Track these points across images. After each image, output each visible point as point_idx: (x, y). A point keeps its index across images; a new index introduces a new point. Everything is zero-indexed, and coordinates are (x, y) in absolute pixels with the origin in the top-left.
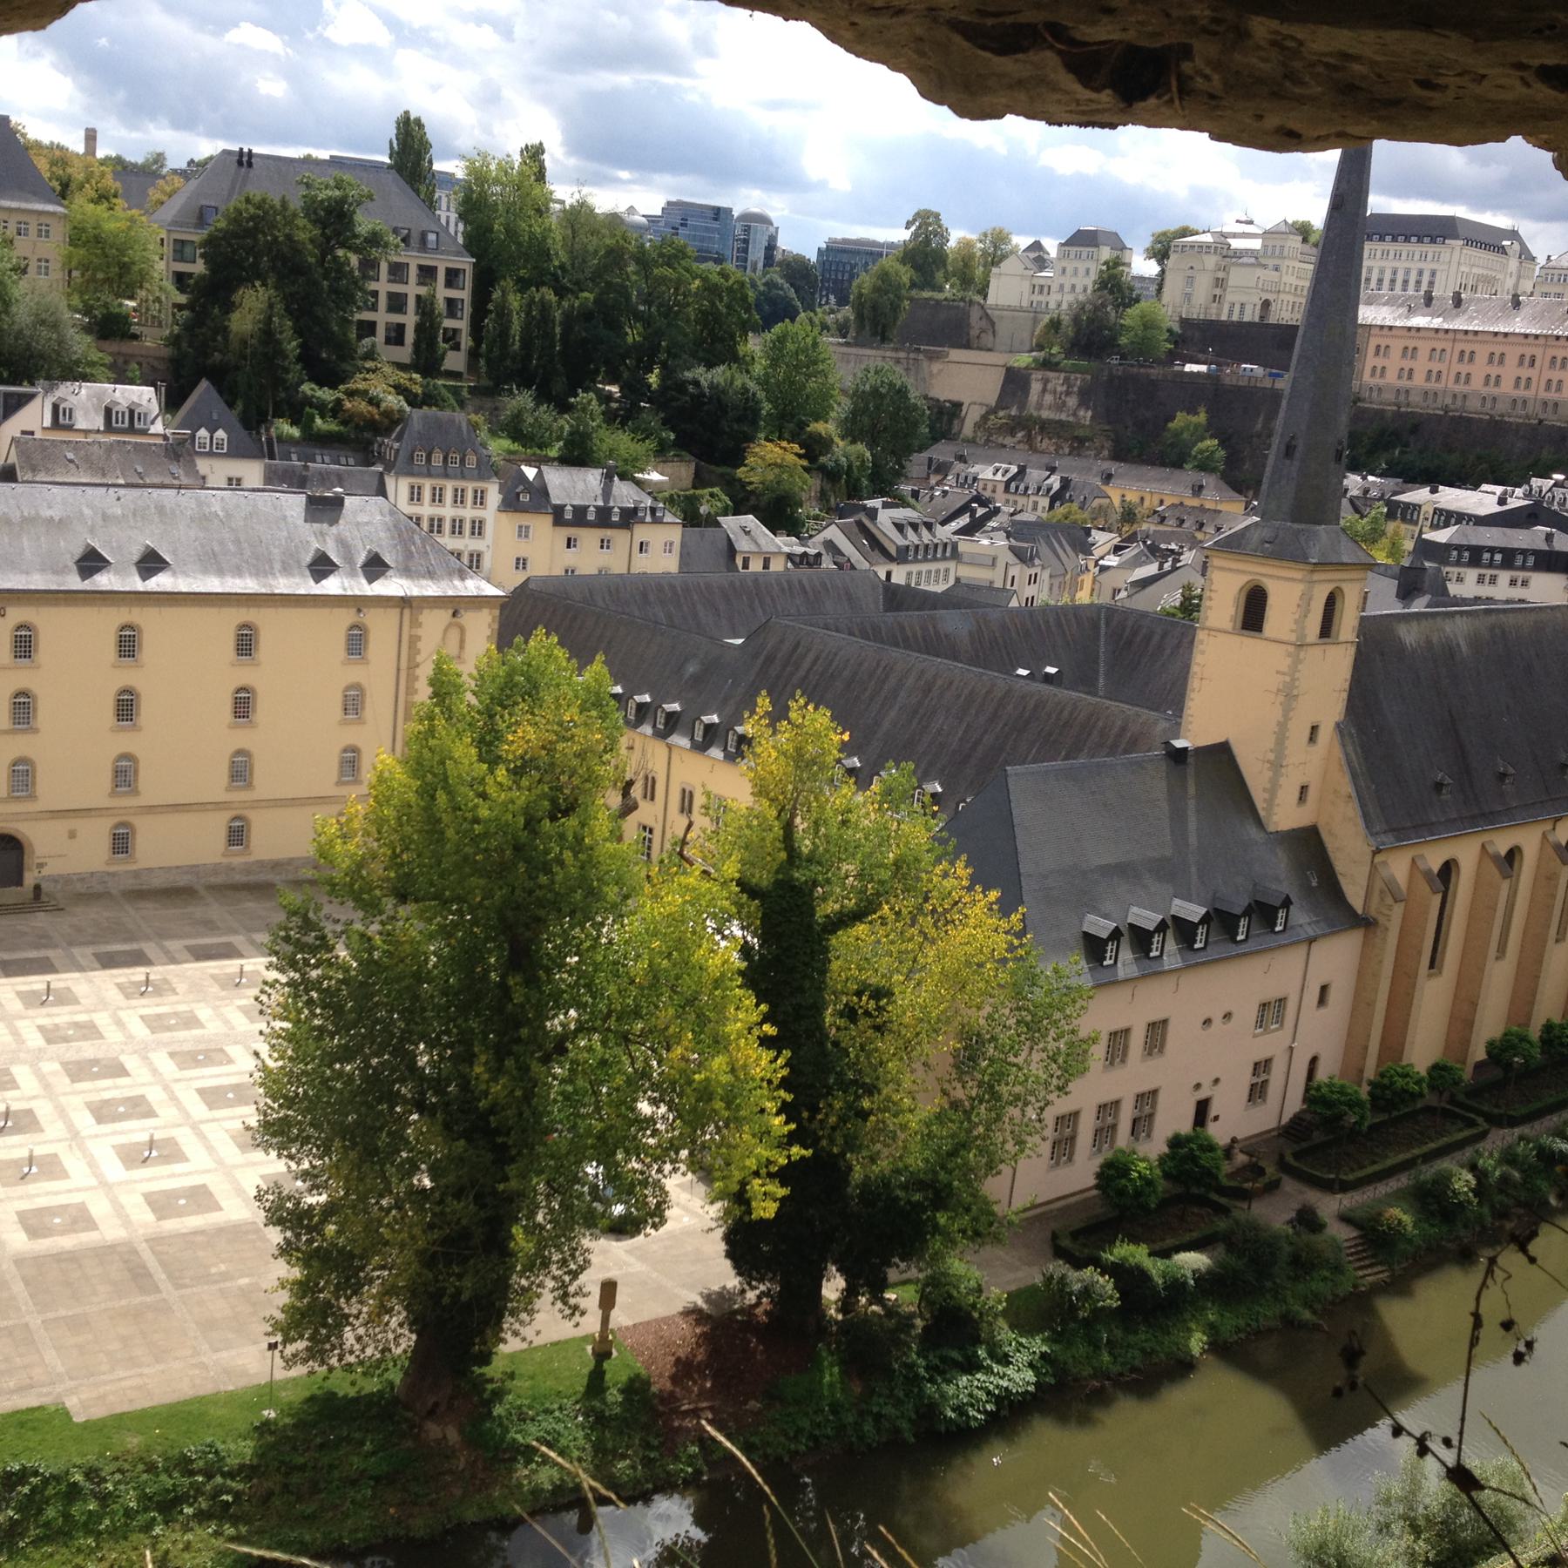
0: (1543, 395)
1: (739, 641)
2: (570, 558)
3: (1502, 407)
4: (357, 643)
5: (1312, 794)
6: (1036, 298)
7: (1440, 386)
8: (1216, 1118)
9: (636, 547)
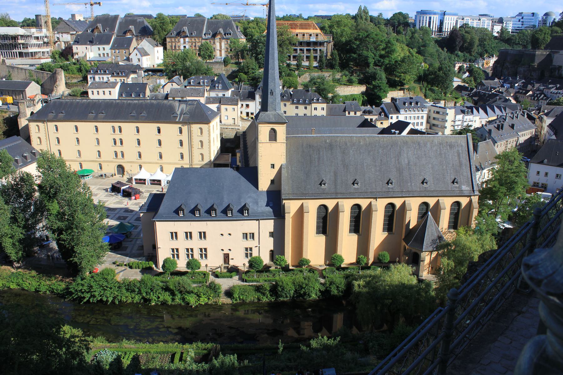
2: (296, 111)
4: (181, 132)
5: (275, 182)
8: (232, 259)
9: (313, 109)
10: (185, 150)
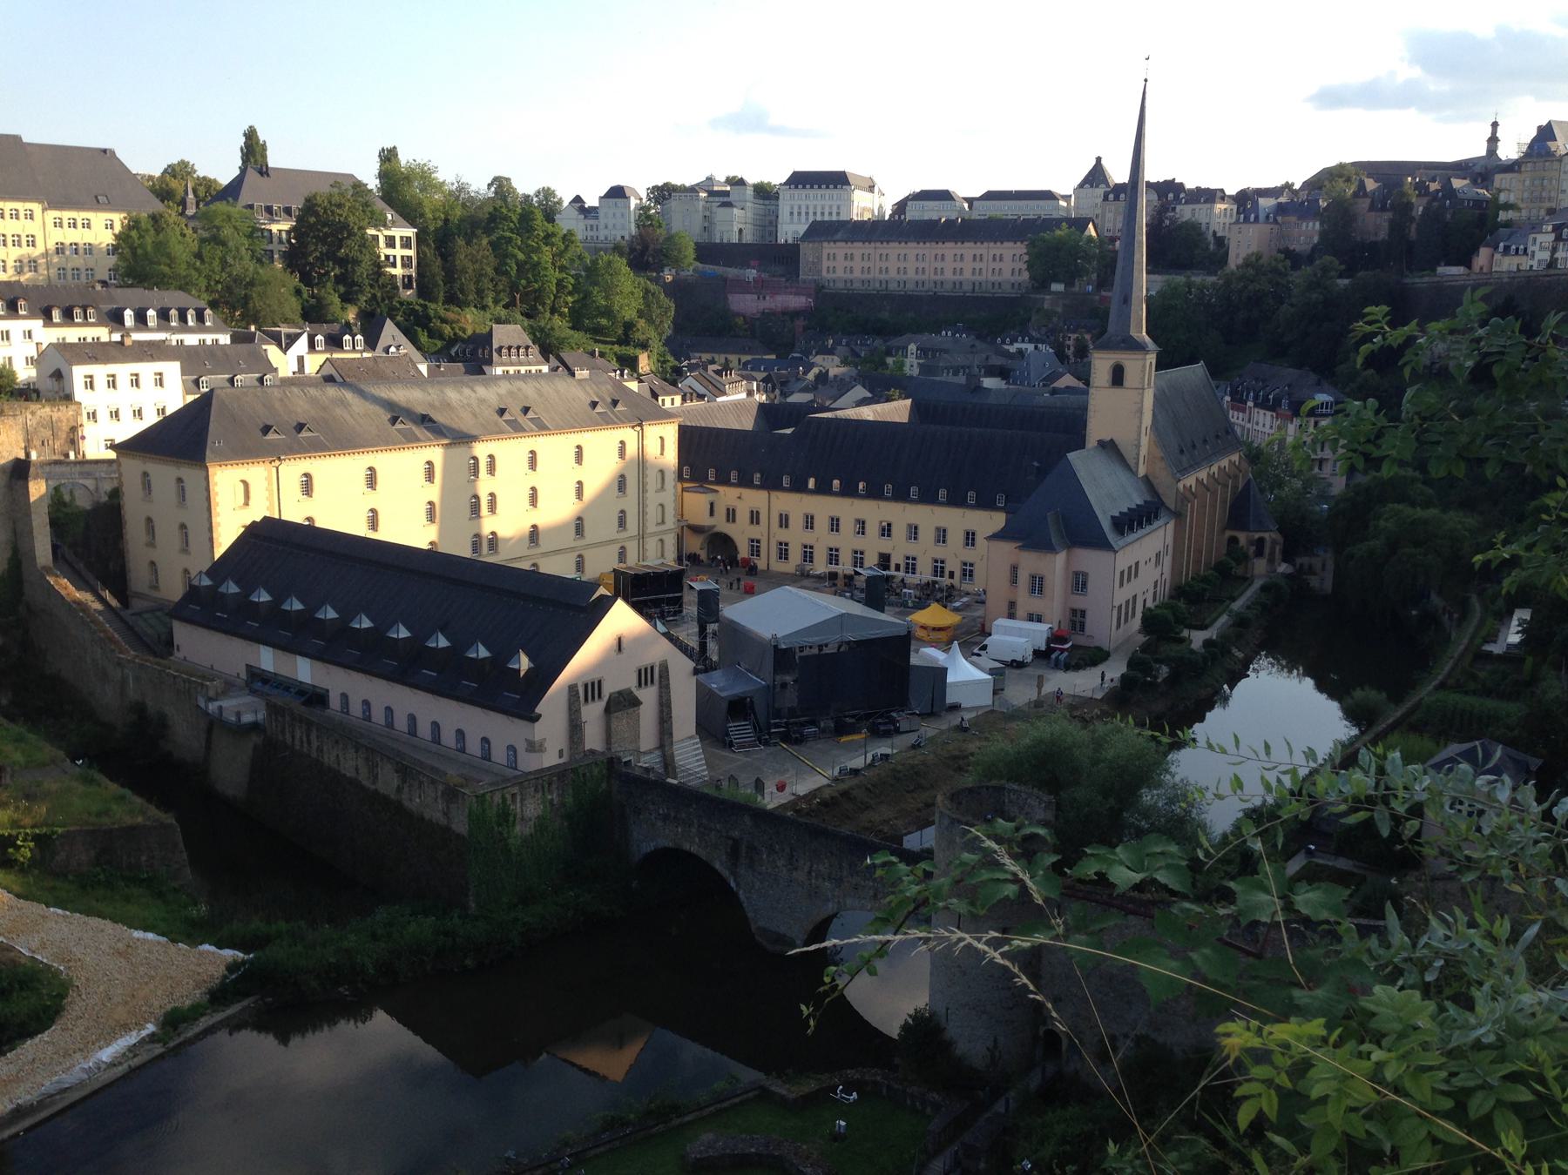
0: (933, 277)
1: (789, 431)
3: (910, 286)
6: (590, 233)
7: (870, 276)
10: (630, 503)
